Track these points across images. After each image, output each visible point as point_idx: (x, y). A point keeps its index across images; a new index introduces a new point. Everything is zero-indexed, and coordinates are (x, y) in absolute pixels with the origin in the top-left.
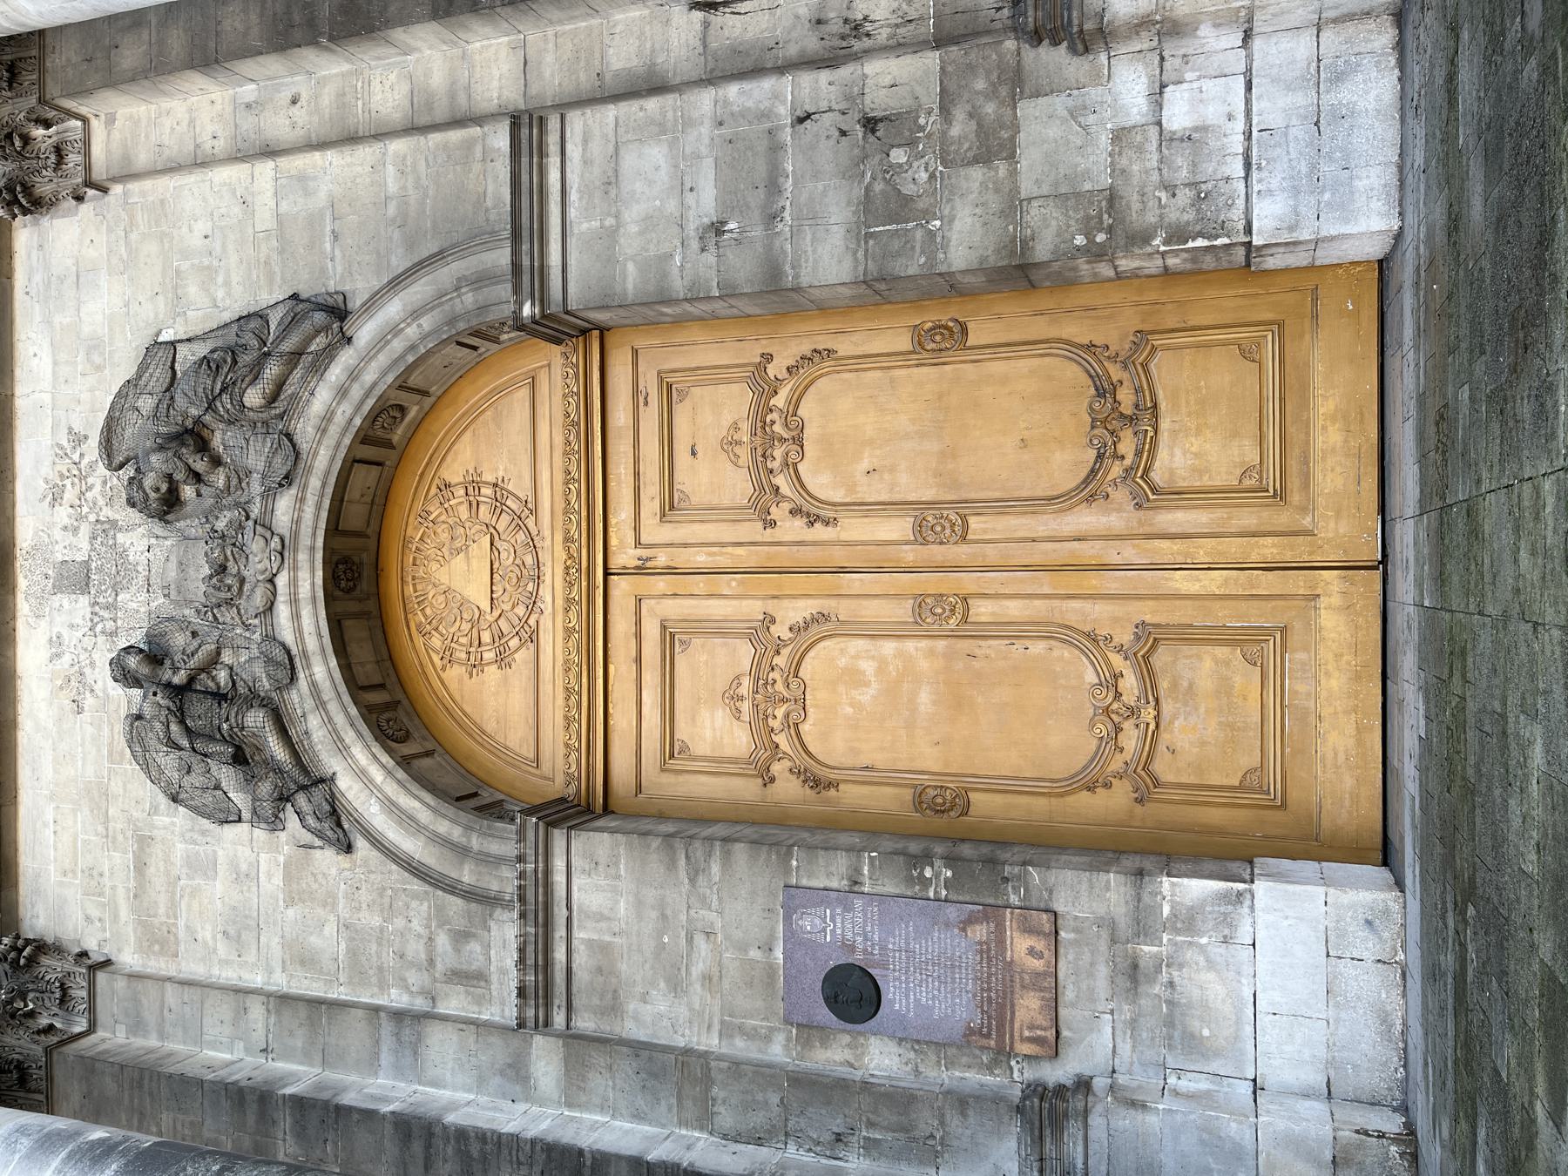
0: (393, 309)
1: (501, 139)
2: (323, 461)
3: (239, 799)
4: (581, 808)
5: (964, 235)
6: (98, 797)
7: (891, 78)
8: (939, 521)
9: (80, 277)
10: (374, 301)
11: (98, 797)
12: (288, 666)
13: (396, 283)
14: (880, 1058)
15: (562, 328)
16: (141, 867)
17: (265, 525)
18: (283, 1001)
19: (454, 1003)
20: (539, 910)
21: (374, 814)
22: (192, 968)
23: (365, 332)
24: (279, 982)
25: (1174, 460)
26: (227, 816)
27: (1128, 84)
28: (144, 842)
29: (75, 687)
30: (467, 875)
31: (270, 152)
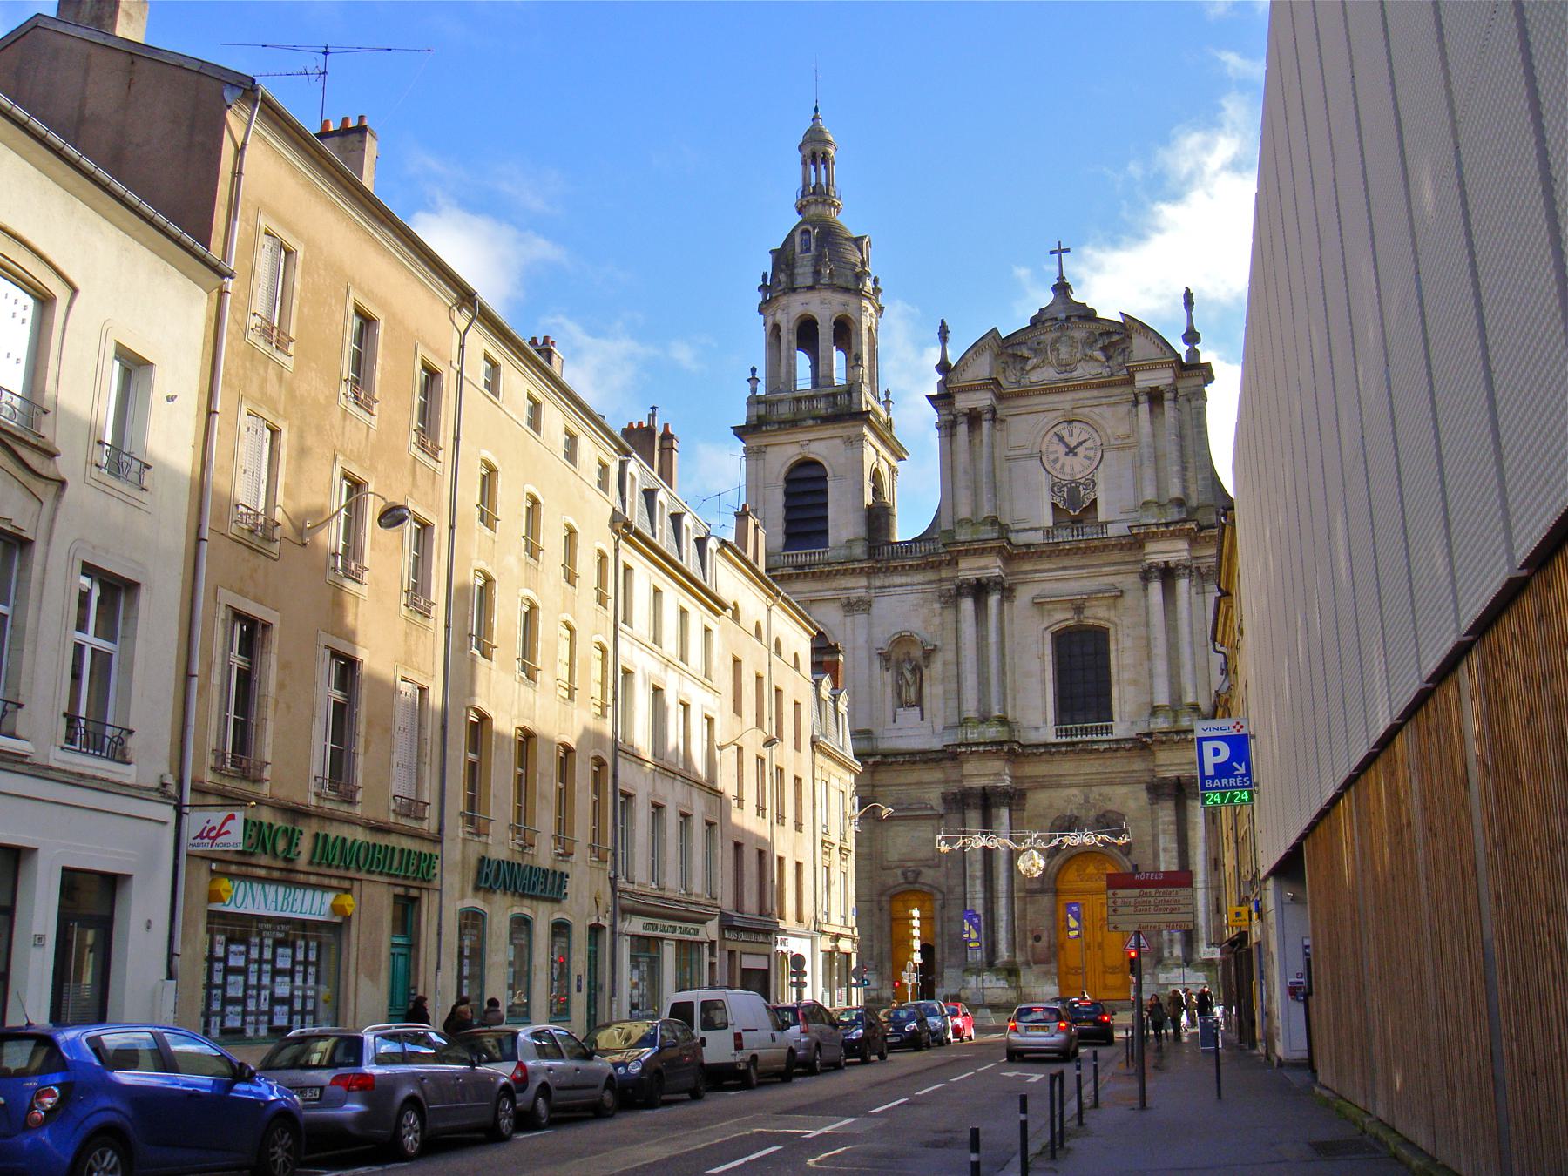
4: (1056, 893)
6: (1051, 806)
7: (1154, 940)
8: (1100, 946)
9: (1136, 799)
11: (1051, 806)
14: (1030, 942)
20: (1042, 891)
25: (1109, 976)
28: (1045, 817)
29: (1068, 801)
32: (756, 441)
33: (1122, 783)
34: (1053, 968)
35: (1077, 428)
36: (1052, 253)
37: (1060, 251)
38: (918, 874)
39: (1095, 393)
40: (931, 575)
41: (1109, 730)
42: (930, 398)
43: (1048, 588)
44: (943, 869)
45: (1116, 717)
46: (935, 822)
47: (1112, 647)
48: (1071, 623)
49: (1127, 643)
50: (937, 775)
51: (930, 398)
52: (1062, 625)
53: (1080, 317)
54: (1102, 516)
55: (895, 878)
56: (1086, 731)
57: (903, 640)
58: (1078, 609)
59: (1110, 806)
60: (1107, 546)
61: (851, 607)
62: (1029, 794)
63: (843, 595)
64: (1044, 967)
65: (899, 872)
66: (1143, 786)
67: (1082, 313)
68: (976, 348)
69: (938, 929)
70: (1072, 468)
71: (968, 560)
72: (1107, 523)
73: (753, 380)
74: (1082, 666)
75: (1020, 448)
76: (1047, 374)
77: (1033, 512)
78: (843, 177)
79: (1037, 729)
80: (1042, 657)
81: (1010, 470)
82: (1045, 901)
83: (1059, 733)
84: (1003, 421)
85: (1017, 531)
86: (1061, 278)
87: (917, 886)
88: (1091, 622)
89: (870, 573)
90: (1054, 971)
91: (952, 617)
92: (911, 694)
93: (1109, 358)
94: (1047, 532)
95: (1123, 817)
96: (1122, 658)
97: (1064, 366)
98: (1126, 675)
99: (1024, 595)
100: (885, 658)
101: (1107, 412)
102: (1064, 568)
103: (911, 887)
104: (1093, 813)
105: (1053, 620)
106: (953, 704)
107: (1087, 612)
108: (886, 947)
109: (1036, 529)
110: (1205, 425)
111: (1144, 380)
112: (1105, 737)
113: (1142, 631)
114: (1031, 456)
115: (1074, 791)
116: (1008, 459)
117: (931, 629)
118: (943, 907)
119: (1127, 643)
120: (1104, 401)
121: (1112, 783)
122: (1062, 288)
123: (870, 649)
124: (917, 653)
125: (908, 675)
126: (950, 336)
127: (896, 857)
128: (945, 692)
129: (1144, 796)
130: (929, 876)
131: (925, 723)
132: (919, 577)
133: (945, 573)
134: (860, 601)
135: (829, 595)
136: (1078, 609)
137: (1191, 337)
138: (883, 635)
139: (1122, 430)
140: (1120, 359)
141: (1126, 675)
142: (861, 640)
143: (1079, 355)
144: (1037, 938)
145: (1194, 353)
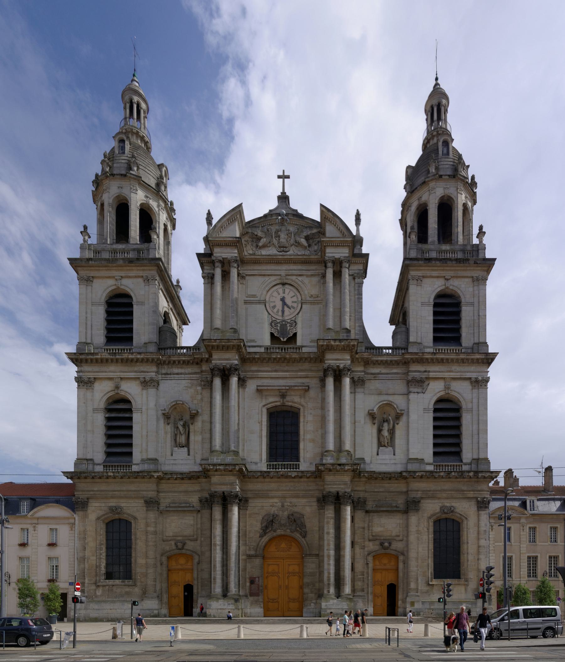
0: (305, 542)
1: (317, 553)
2: (293, 535)
3: (263, 525)
4: (264, 558)
5: (306, 590)
7: (317, 585)
10: (305, 540)
12: (275, 531)
13: (307, 543)
15: (303, 558)
16: (256, 514)
17: (288, 529)
18: (246, 532)
19: (247, 547)
20: (256, 556)
21: (263, 540)
22: (248, 519)
23: (303, 540)
24: (247, 530)
26: (261, 524)
27: (314, 601)
30: (258, 549)
31: (319, 530)
32: (85, 273)
33: (303, 497)
34: (260, 598)
38: (184, 544)
39: (299, 267)
40: (196, 369)
41: (297, 466)
43: (266, 382)
44: (199, 542)
45: (301, 459)
46: (195, 515)
47: (302, 420)
48: (278, 404)
49: (310, 418)
50: (197, 487)
52: (273, 404)
53: (294, 215)
54: (299, 342)
55: (170, 547)
56: (284, 466)
57: (177, 406)
58: (283, 396)
59: (295, 509)
60: (302, 359)
61: (146, 384)
62: (250, 501)
63: (142, 375)
64: (256, 598)
65: (173, 543)
66: (315, 499)
67: (295, 213)
69: (195, 576)
71: (220, 362)
72: (303, 347)
73: (85, 231)
74: (283, 429)
75: (254, 296)
76: (272, 251)
77: (259, 335)
79: (256, 463)
80: (261, 423)
81: (246, 309)
82: (257, 561)
83: (269, 466)
84: (243, 278)
85: (249, 347)
87: (184, 551)
88: (290, 404)
89: (159, 364)
90: (261, 600)
91: (209, 394)
92: (183, 439)
93: (309, 246)
94: (267, 348)
95: (303, 516)
96: (307, 427)
97: (283, 248)
98: (308, 436)
99: (252, 385)
100: (167, 417)
101: (306, 280)
102: (276, 371)
103: (180, 551)
104: (286, 513)
105: (268, 402)
106: (207, 446)
107: (288, 398)
108: (165, 585)
109: (260, 347)
110: (362, 295)
112: (295, 470)
113: (319, 412)
114: (259, 302)
115: (276, 500)
116: (246, 302)
117: (195, 402)
118: (198, 563)
119: (310, 418)
120: (304, 272)
121: (297, 497)
123: (157, 411)
124: (187, 417)
125: (181, 428)
127: (171, 534)
128: (203, 439)
129: (315, 504)
130: (190, 545)
131: (190, 457)
132: (189, 370)
133: (205, 367)
134: (152, 380)
135: (132, 375)
136: (283, 396)
138: (165, 402)
139: (314, 292)
140: (316, 248)
141: (308, 436)
142: (152, 404)
143: (292, 241)
144: (252, 582)
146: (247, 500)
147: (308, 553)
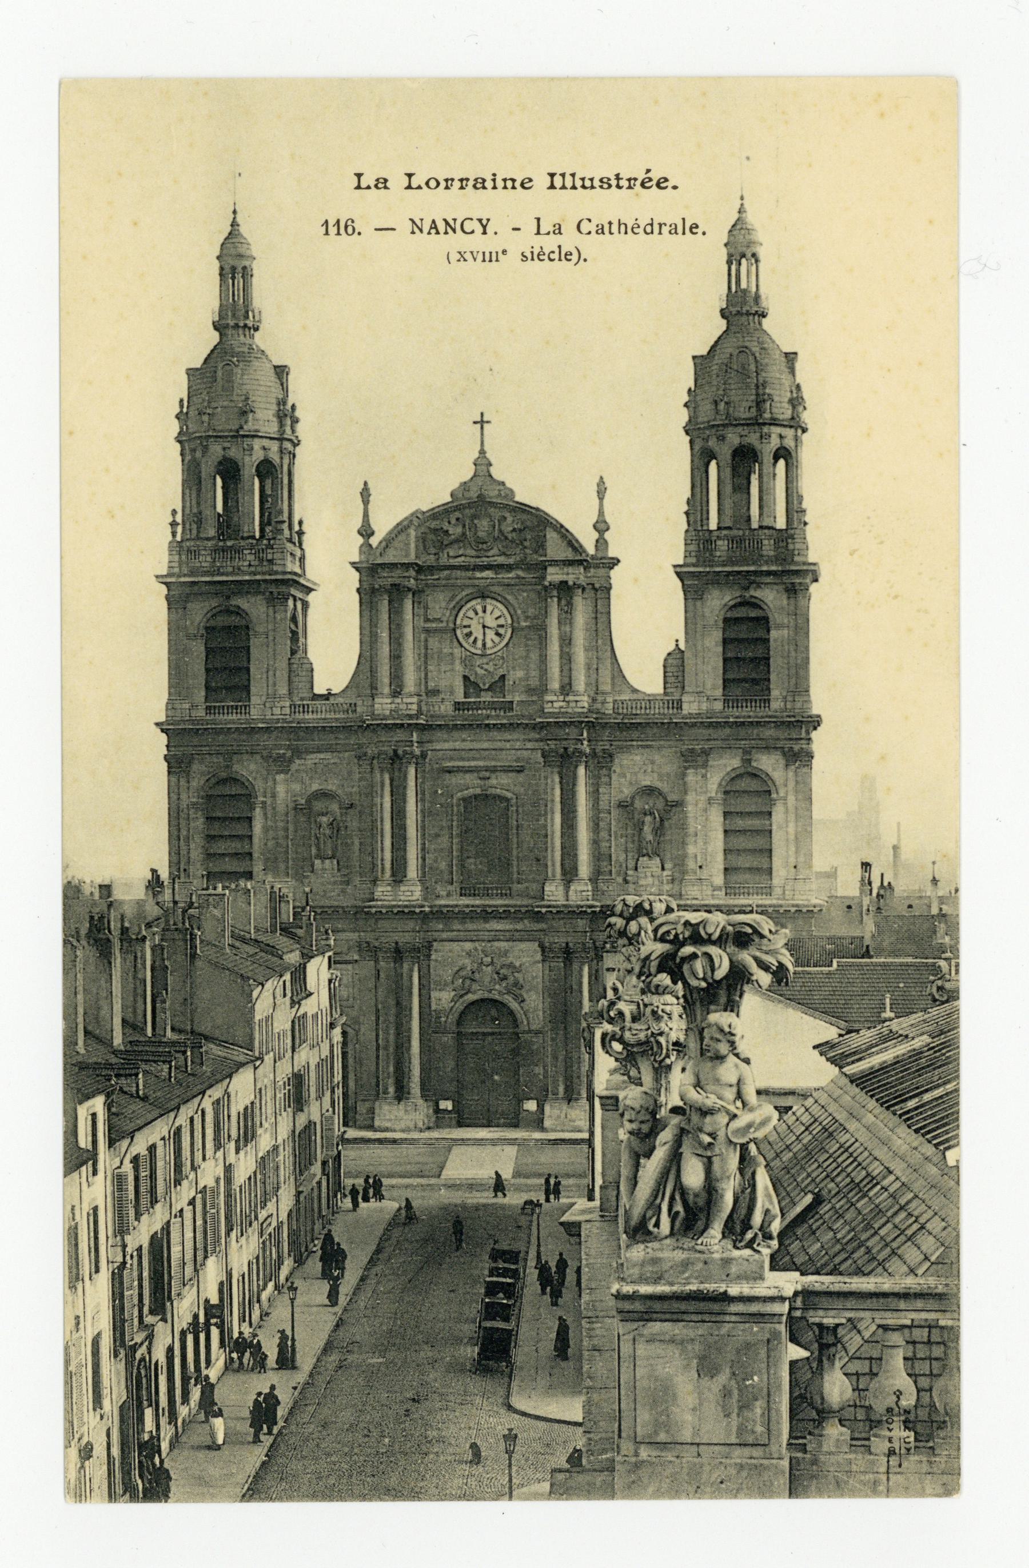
35: (490, 604)
36: (475, 423)
37: (482, 422)
42: (353, 564)
51: (353, 564)
68: (401, 529)
70: (484, 645)
75: (440, 620)
78: (265, 294)
86: (482, 452)
94: (458, 706)
111: (554, 575)
122: (482, 463)
126: (371, 498)
137: (601, 526)
145: (601, 543)
146: (429, 946)
147: (526, 1028)
